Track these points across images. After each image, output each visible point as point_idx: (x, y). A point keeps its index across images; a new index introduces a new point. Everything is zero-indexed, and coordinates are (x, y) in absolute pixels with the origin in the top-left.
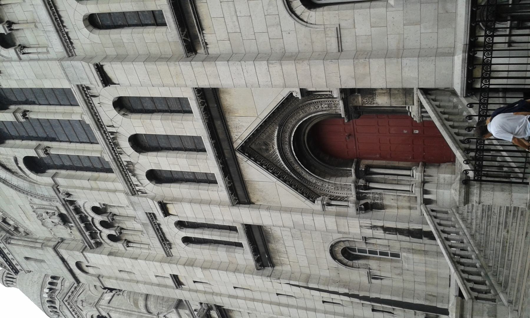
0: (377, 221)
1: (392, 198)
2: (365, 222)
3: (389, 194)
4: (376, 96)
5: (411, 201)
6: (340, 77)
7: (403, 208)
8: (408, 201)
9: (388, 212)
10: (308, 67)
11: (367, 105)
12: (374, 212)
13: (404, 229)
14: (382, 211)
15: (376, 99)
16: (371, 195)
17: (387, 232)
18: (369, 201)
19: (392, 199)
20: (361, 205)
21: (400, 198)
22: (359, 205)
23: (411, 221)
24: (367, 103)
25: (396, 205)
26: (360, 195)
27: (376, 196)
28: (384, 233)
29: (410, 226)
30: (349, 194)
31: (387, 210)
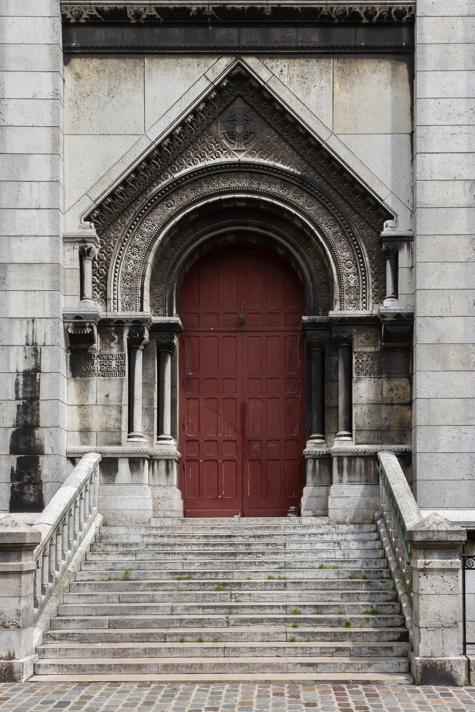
4: (376, 380)
5: (105, 433)
6: (440, 316)
7: (84, 416)
10: (462, 259)
11: (354, 361)
15: (369, 379)
16: (115, 351)
18: (97, 345)
19: (107, 396)
21: (114, 413)
24: (360, 361)
26: (113, 329)
28: (17, 372)
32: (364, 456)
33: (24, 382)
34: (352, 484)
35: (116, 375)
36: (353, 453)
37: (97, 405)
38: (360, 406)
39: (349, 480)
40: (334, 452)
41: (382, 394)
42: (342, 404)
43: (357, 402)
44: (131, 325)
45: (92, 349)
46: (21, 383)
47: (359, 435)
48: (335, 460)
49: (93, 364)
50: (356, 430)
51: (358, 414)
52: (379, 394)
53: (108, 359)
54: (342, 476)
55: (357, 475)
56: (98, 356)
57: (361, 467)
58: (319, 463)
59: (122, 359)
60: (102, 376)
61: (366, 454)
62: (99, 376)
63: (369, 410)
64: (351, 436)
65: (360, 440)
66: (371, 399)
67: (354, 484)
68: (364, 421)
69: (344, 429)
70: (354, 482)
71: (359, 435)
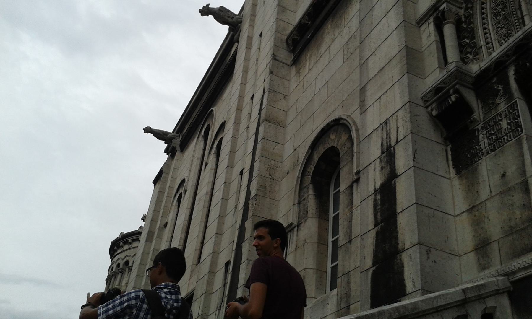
0: (410, 151)
1: (509, 173)
2: (400, 123)
3: (522, 155)
8: (511, 227)
9: (452, 186)
12: (443, 147)
13: (396, 238)
14: (452, 171)
17: (379, 197)
18: (479, 114)
19: (504, 175)
20: (457, 91)
22: (457, 86)
23: (428, 252)
25: (484, 194)
26: (495, 79)
27: (504, 124)
28: (376, 191)
29: (410, 252)
30: (488, 48)
31: (456, 182)
33: (381, 200)
35: (510, 138)
37: (492, 197)
44: (514, 58)
45: (472, 122)
46: (379, 202)
49: (479, 142)
53: (495, 122)
56: (482, 128)
59: (514, 110)
60: (492, 151)
62: (488, 153)
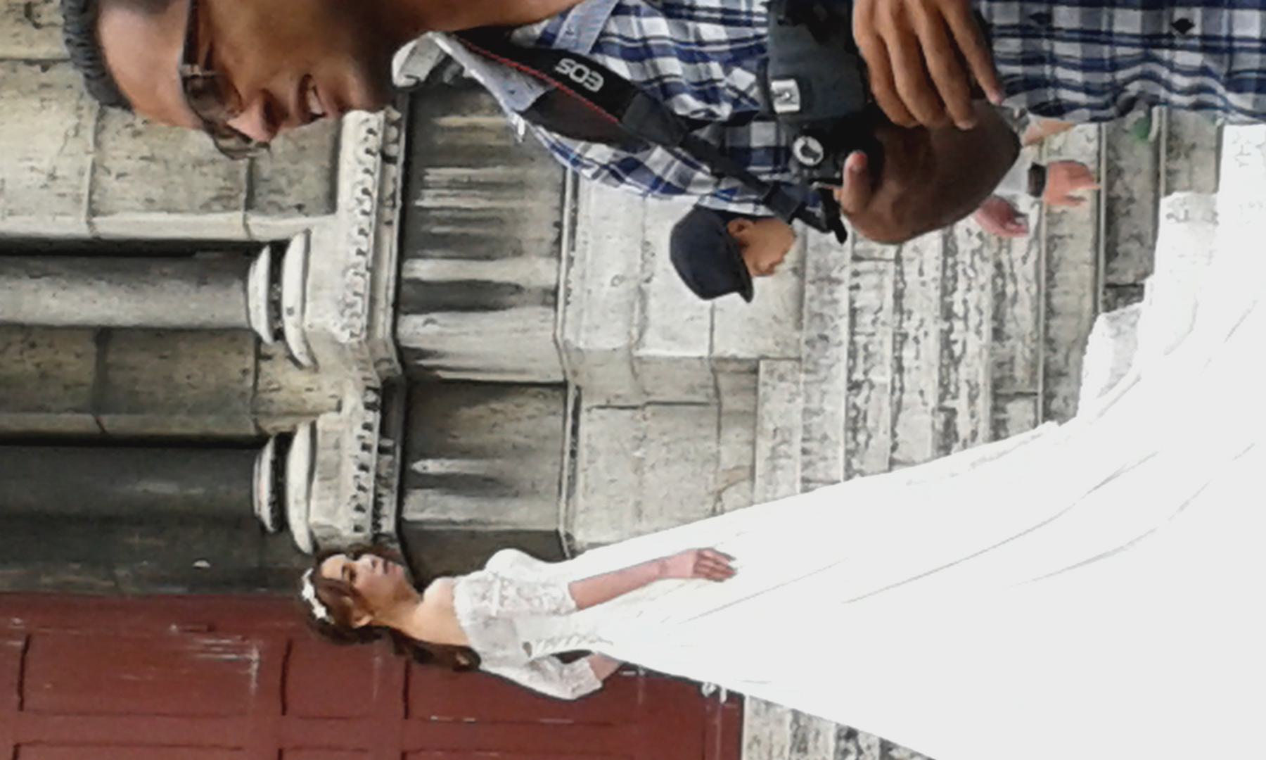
32: (407, 165)
34: (573, 234)
36: (381, 222)
38: (109, 182)
39: (546, 247)
40: (370, 327)
41: (45, 65)
42: (88, 292)
43: (77, 199)
47: (280, 191)
48: (417, 329)
50: (249, 205)
51: (156, 193)
52: (45, 77)
54: (517, 289)
55: (515, 204)
57: (471, 185)
58: (436, 455)
61: (398, 150)
63: (137, 134)
64: (279, 249)
65: (313, 186)
66: (72, 121)
67: (574, 222)
68: (198, 163)
69: (237, 285)
70: (559, 225)
71: (280, 191)
